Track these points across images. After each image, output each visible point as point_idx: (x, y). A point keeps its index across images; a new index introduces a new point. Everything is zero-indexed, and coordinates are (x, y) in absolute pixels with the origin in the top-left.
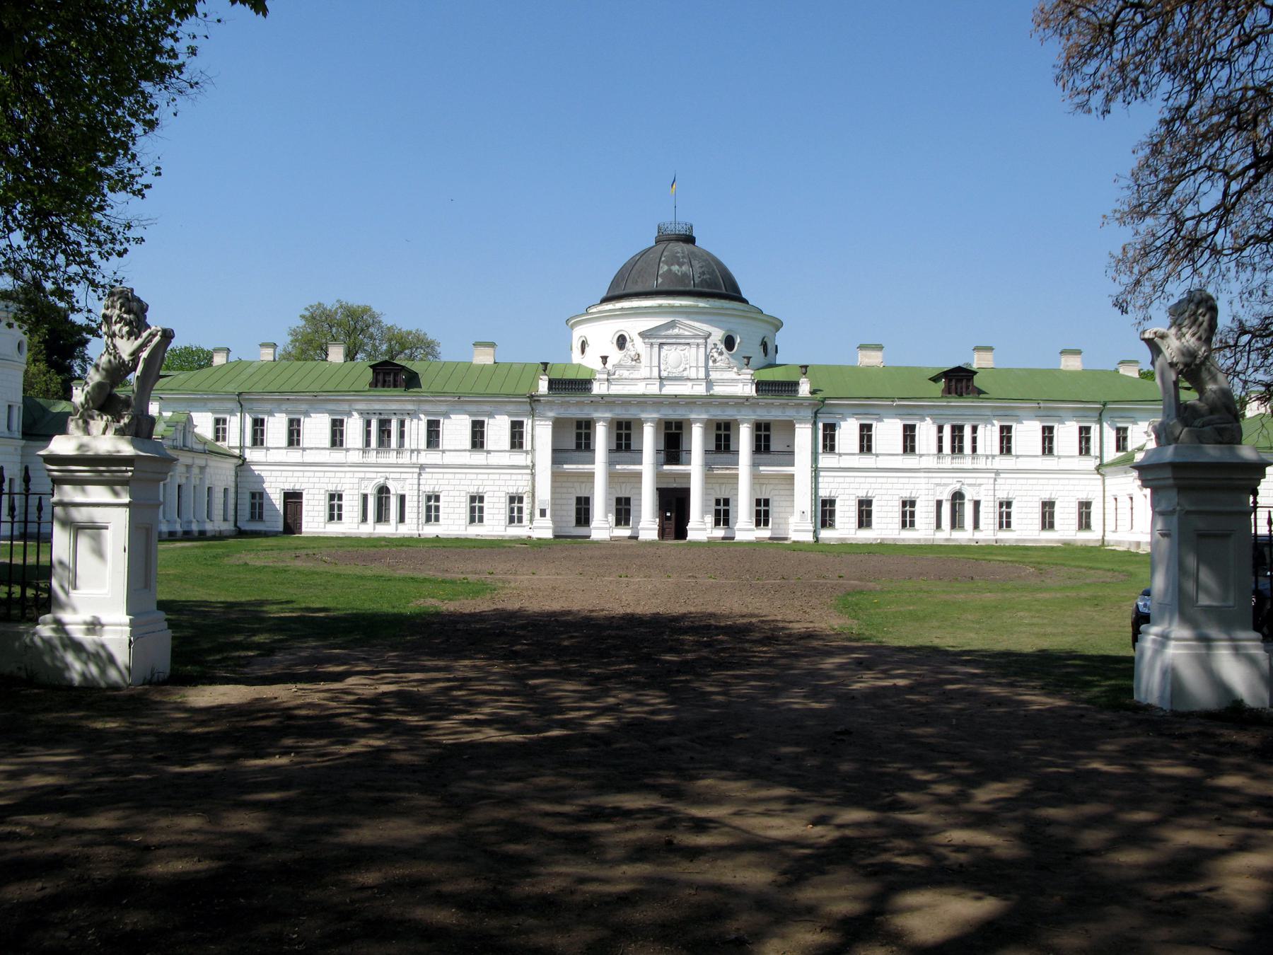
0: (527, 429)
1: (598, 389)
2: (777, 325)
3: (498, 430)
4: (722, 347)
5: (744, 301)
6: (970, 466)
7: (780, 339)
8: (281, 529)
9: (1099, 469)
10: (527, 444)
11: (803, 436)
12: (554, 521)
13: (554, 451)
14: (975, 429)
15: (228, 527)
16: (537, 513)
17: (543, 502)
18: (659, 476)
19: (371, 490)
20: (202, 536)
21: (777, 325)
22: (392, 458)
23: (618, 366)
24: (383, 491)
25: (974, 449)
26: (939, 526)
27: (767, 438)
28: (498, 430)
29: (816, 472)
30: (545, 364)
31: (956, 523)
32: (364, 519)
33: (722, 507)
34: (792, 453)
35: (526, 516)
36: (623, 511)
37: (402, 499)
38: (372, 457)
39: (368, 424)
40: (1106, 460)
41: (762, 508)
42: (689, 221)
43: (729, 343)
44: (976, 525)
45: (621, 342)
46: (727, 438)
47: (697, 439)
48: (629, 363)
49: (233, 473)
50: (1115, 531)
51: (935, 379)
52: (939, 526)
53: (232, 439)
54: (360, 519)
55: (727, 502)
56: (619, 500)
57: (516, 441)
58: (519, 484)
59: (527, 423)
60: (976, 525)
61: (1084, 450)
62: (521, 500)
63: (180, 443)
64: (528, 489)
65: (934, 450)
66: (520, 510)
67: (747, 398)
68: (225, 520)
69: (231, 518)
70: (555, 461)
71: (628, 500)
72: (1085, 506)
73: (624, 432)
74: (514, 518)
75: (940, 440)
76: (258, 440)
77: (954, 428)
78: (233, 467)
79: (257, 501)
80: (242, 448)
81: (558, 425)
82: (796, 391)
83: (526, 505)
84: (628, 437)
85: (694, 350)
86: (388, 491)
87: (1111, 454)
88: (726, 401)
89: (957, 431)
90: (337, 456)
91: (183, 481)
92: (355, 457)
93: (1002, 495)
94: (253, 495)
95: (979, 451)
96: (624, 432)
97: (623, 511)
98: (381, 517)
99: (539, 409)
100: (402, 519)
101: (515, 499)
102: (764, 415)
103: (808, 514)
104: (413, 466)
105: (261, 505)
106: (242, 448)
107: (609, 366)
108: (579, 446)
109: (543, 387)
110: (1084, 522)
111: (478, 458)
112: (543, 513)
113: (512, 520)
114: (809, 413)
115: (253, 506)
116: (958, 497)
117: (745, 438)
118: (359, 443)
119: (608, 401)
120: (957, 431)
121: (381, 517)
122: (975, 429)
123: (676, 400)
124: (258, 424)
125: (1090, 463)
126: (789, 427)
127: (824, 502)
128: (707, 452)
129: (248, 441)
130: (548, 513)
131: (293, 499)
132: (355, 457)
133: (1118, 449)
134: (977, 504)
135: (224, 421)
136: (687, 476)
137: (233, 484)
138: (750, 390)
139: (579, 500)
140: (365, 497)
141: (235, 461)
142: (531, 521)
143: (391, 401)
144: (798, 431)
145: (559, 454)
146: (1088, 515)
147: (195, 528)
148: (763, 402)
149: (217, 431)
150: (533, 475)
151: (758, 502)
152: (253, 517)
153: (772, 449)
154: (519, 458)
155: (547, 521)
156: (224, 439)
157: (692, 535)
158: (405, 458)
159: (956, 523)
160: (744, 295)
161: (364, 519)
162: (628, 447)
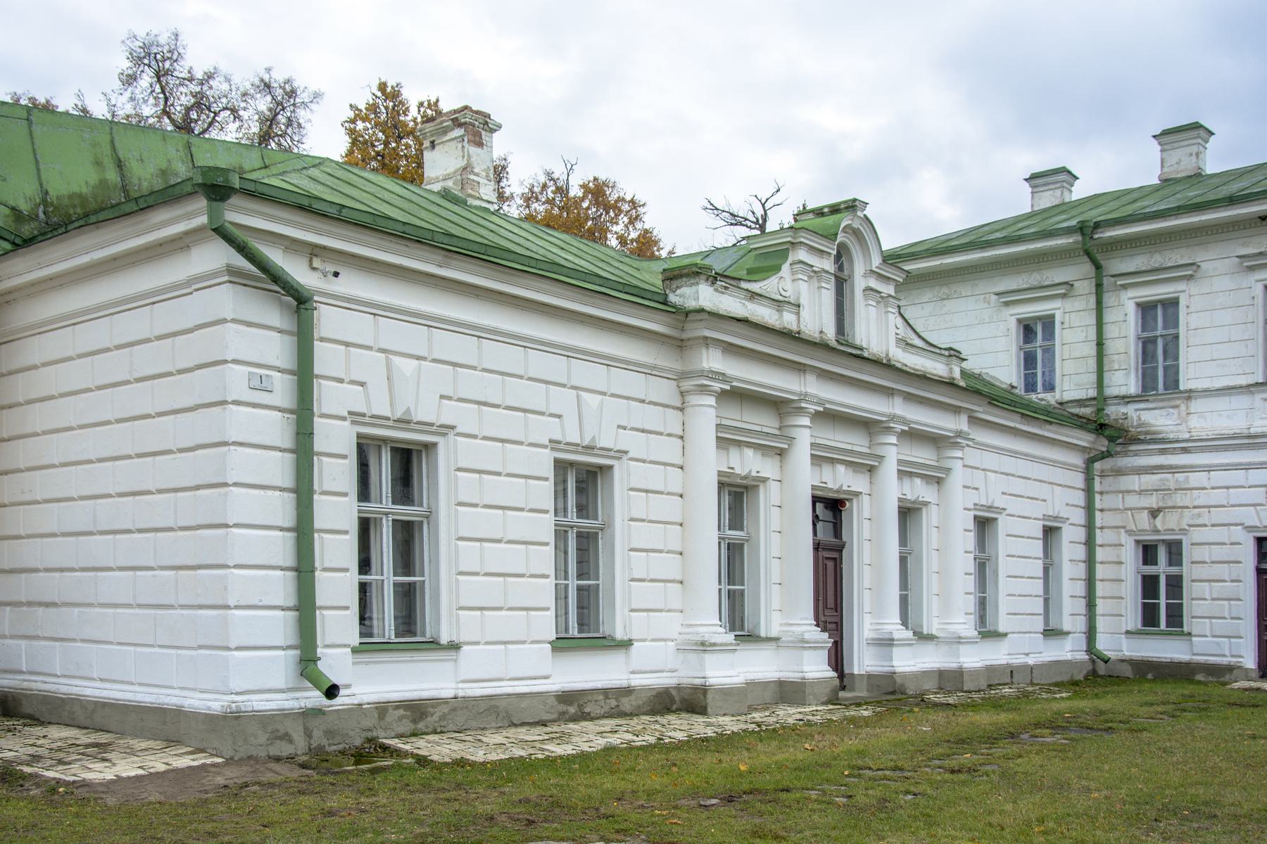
15: (1070, 650)
49: (1078, 480)
69: (1071, 619)
78: (1077, 460)
79: (1162, 568)
80: (1101, 400)
91: (839, 479)
94: (1148, 552)
105: (1175, 584)
106: (1101, 400)
115: (1149, 585)
124: (1159, 317)
129: (1124, 380)
135: (1048, 322)
137: (1078, 516)
141: (1083, 439)
149: (1029, 361)
152: (1149, 616)
156: (1050, 387)
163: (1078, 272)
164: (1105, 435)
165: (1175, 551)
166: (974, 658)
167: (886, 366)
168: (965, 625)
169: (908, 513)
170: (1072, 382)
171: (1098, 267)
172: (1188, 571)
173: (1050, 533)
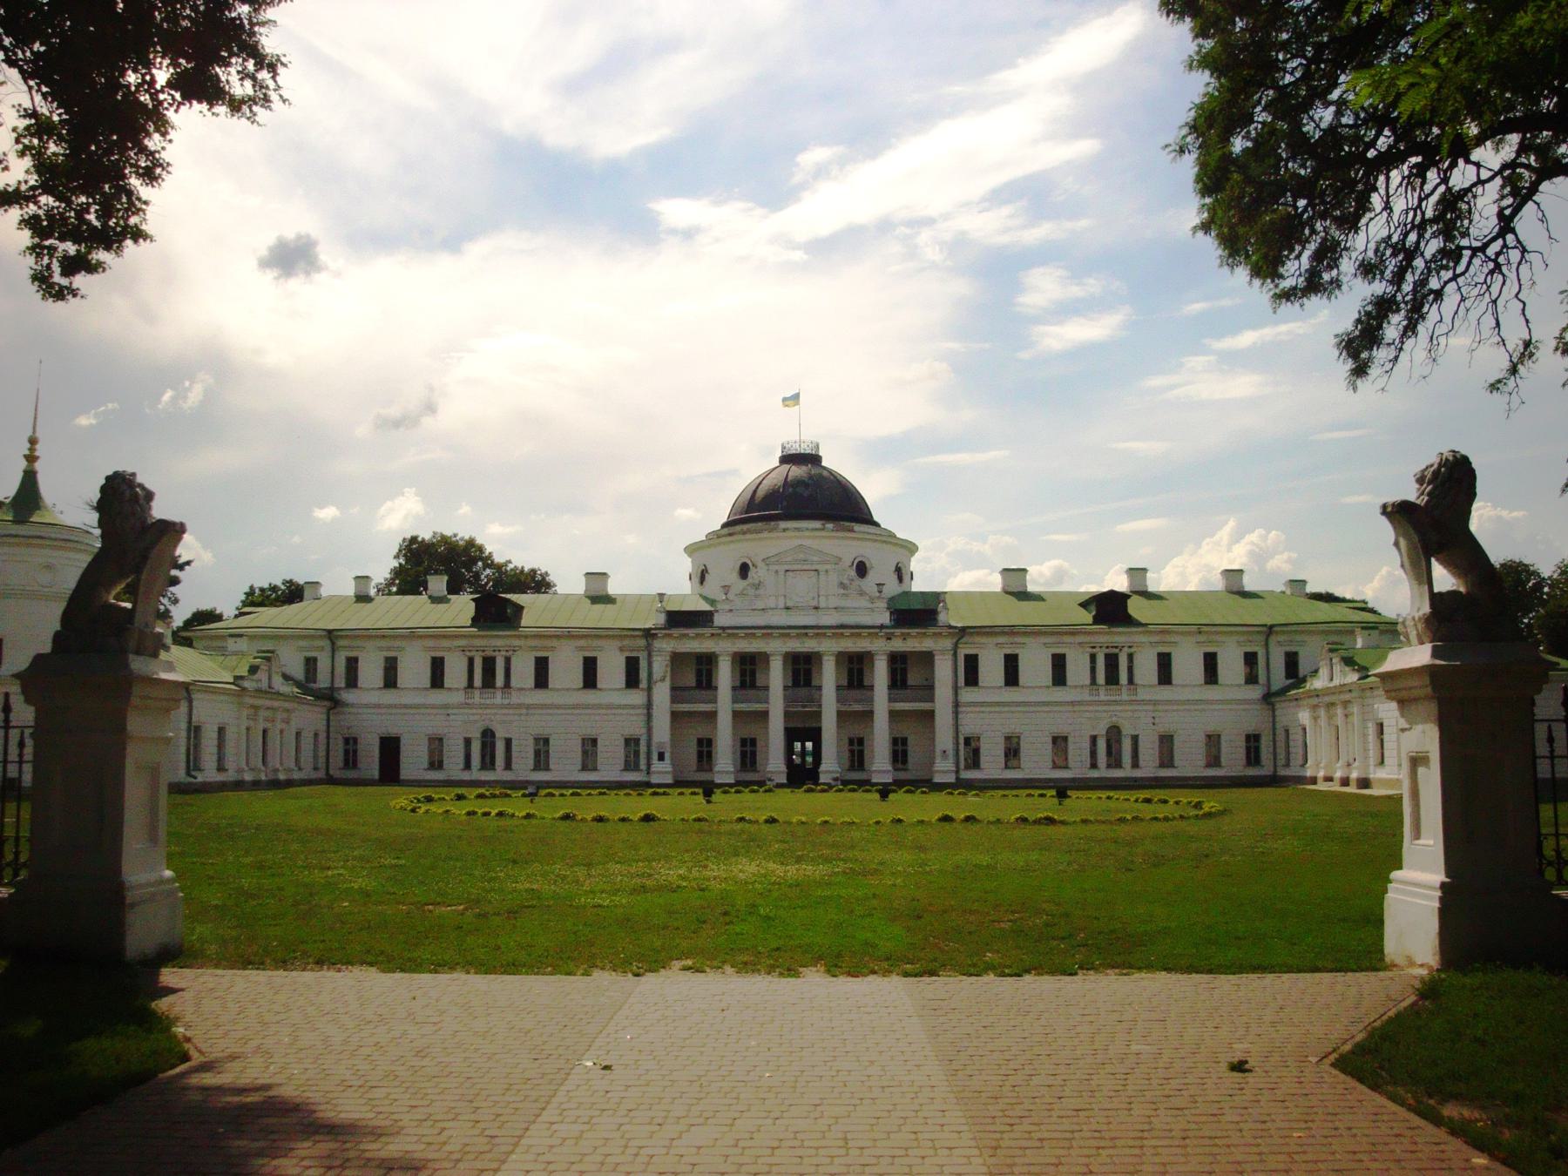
0: (643, 664)
1: (719, 620)
2: (911, 548)
3: (612, 669)
4: (853, 573)
5: (877, 524)
6: (1125, 697)
7: (915, 564)
8: (377, 776)
9: (1269, 698)
10: (644, 685)
11: (944, 672)
12: (673, 765)
13: (673, 689)
14: (1131, 657)
15: (321, 774)
16: (655, 756)
17: (661, 744)
18: (787, 715)
19: (476, 735)
20: (289, 783)
21: (911, 548)
22: (498, 698)
23: (742, 594)
24: (488, 736)
25: (1131, 681)
26: (1094, 766)
27: (904, 672)
28: (612, 669)
29: (957, 705)
30: (661, 595)
31: (1115, 762)
32: (468, 766)
33: (856, 748)
34: (930, 688)
35: (643, 762)
36: (748, 753)
37: (508, 742)
38: (477, 697)
39: (471, 661)
40: (1275, 687)
41: (900, 748)
42: (815, 440)
43: (862, 569)
44: (1135, 765)
45: (744, 570)
46: (861, 672)
47: (829, 677)
48: (751, 592)
50: (1287, 765)
51: (1084, 605)
52: (1094, 766)
53: (323, 681)
54: (462, 766)
55: (861, 741)
56: (744, 742)
57: (632, 681)
58: (636, 728)
59: (643, 656)
60: (1135, 765)
61: (1251, 679)
62: (637, 741)
63: (264, 685)
64: (644, 731)
65: (1088, 682)
66: (637, 754)
67: (882, 627)
68: (316, 769)
70: (674, 700)
71: (753, 742)
72: (1253, 740)
73: (748, 667)
74: (631, 764)
75: (1093, 670)
76: (352, 681)
77: (1107, 656)
80: (332, 689)
81: (677, 659)
82: (935, 620)
83: (643, 748)
84: (753, 673)
85: (822, 577)
86: (493, 734)
87: (1279, 678)
88: (857, 629)
89: (1112, 662)
90: (437, 697)
92: (458, 697)
93: (1162, 728)
94: (347, 741)
95: (1137, 679)
96: (748, 667)
97: (748, 753)
98: (488, 762)
99: (657, 644)
100: (508, 765)
101: (631, 743)
102: (898, 645)
103: (951, 753)
104: (520, 706)
105: (355, 752)
106: (332, 689)
107: (731, 596)
108: (699, 686)
109: (661, 619)
110: (1253, 756)
111: (590, 697)
112: (661, 757)
113: (627, 763)
114: (948, 643)
115: (346, 752)
116: (1114, 733)
117: (880, 675)
118: (464, 683)
119: (729, 632)
120: (1112, 662)
121: (488, 762)
122: (1131, 657)
123: (804, 631)
124: (352, 663)
125: (1256, 692)
126: (927, 658)
127: (967, 741)
128: (839, 688)
129: (340, 682)
130: (667, 756)
131: (390, 747)
132: (458, 697)
133: (1287, 677)
134: (1135, 739)
136: (818, 715)
138: (885, 618)
139: (700, 741)
140: (468, 742)
141: (327, 703)
142: (649, 765)
143: (496, 641)
144: (937, 663)
145: (677, 692)
146: (1257, 750)
147: (282, 777)
148: (898, 631)
150: (649, 716)
151: (895, 741)
153: (910, 682)
154: (636, 697)
155: (666, 766)
157: (823, 778)
158: (515, 698)
159: (1115, 762)
160: (876, 518)
161: (468, 765)
162: (753, 686)
163: (326, 643)
164: (330, 700)
165: (355, 740)
166: (296, 776)
167: (278, 693)
168: (292, 765)
169: (282, 732)
170: (323, 681)
171: (333, 644)
172: (359, 747)
173: (316, 735)
